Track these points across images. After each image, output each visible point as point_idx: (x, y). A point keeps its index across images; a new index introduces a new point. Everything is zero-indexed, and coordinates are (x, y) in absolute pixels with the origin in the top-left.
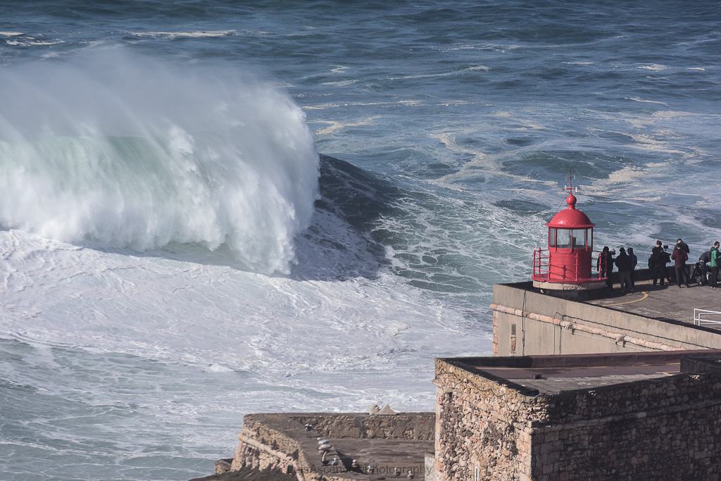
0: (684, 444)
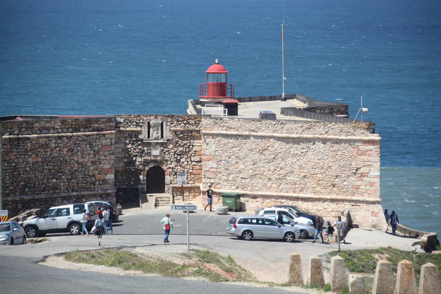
0: (70, 154)
